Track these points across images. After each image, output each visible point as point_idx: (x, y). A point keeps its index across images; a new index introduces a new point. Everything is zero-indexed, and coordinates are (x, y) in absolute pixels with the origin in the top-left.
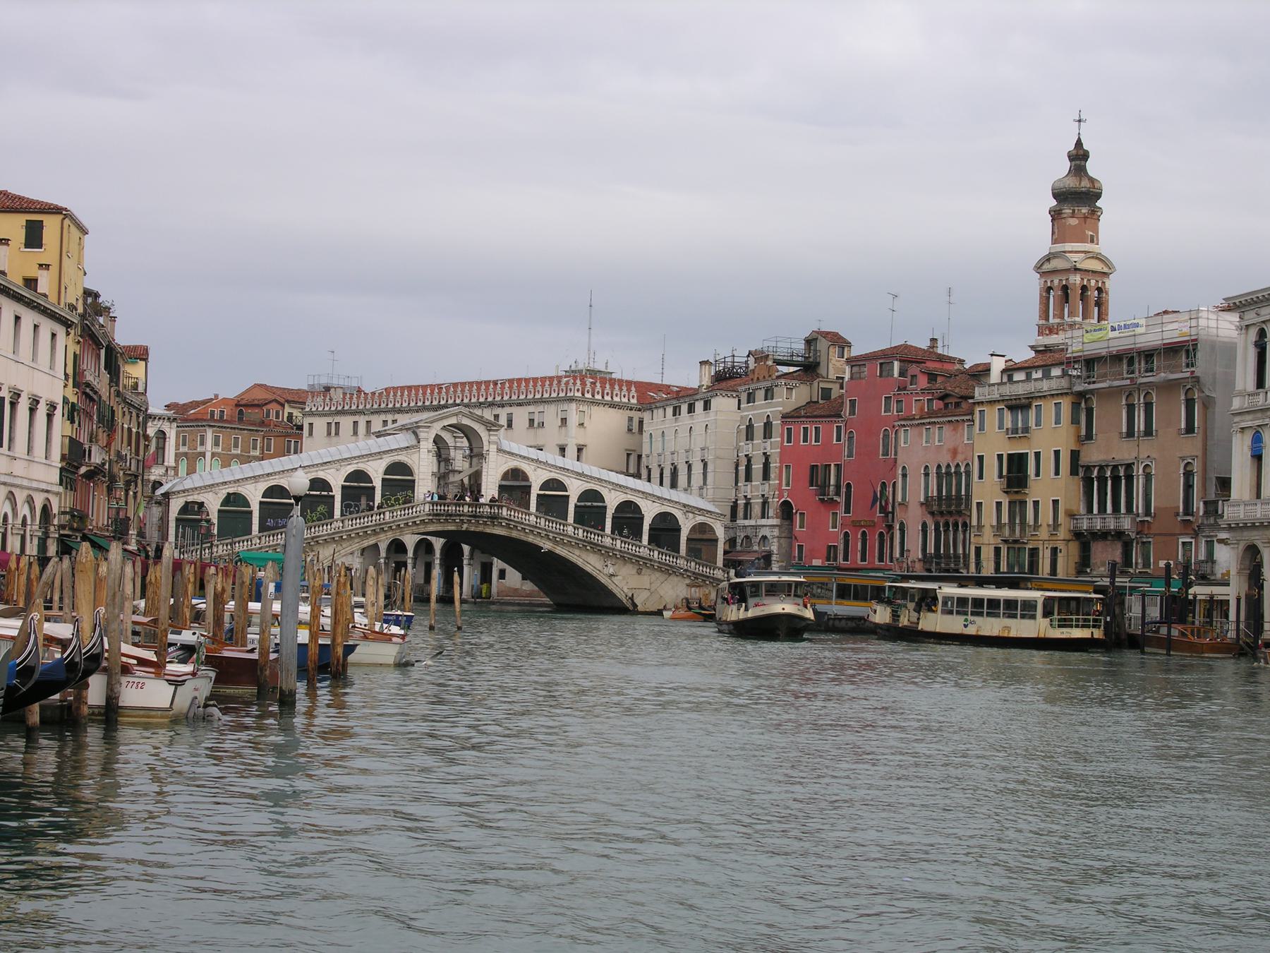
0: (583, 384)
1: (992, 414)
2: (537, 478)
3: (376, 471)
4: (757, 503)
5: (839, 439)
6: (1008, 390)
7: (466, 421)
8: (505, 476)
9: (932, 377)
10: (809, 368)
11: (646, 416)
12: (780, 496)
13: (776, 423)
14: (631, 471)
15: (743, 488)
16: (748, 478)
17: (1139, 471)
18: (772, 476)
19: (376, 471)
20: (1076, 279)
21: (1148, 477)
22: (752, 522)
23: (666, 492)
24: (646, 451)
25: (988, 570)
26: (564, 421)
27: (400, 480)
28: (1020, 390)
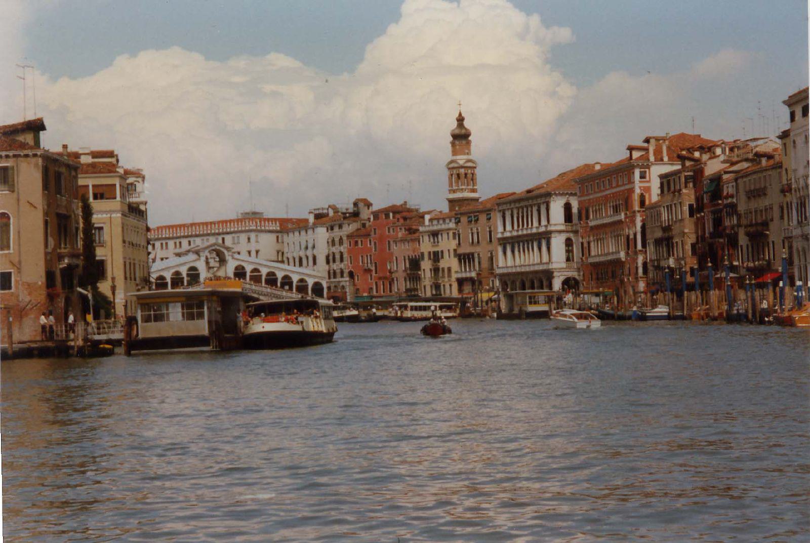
0: (256, 223)
1: (426, 238)
2: (249, 268)
3: (184, 271)
4: (338, 271)
5: (370, 245)
6: (431, 228)
7: (218, 248)
8: (236, 268)
9: (405, 219)
10: (356, 215)
11: (285, 236)
12: (349, 268)
13: (345, 238)
14: (280, 259)
15: (332, 266)
16: (334, 261)
17: (476, 255)
18: (344, 260)
19: (184, 271)
20: (462, 171)
21: (479, 258)
22: (337, 280)
23: (297, 269)
24: (286, 250)
25: (429, 294)
26: (249, 239)
27: (194, 275)
28: (435, 228)
